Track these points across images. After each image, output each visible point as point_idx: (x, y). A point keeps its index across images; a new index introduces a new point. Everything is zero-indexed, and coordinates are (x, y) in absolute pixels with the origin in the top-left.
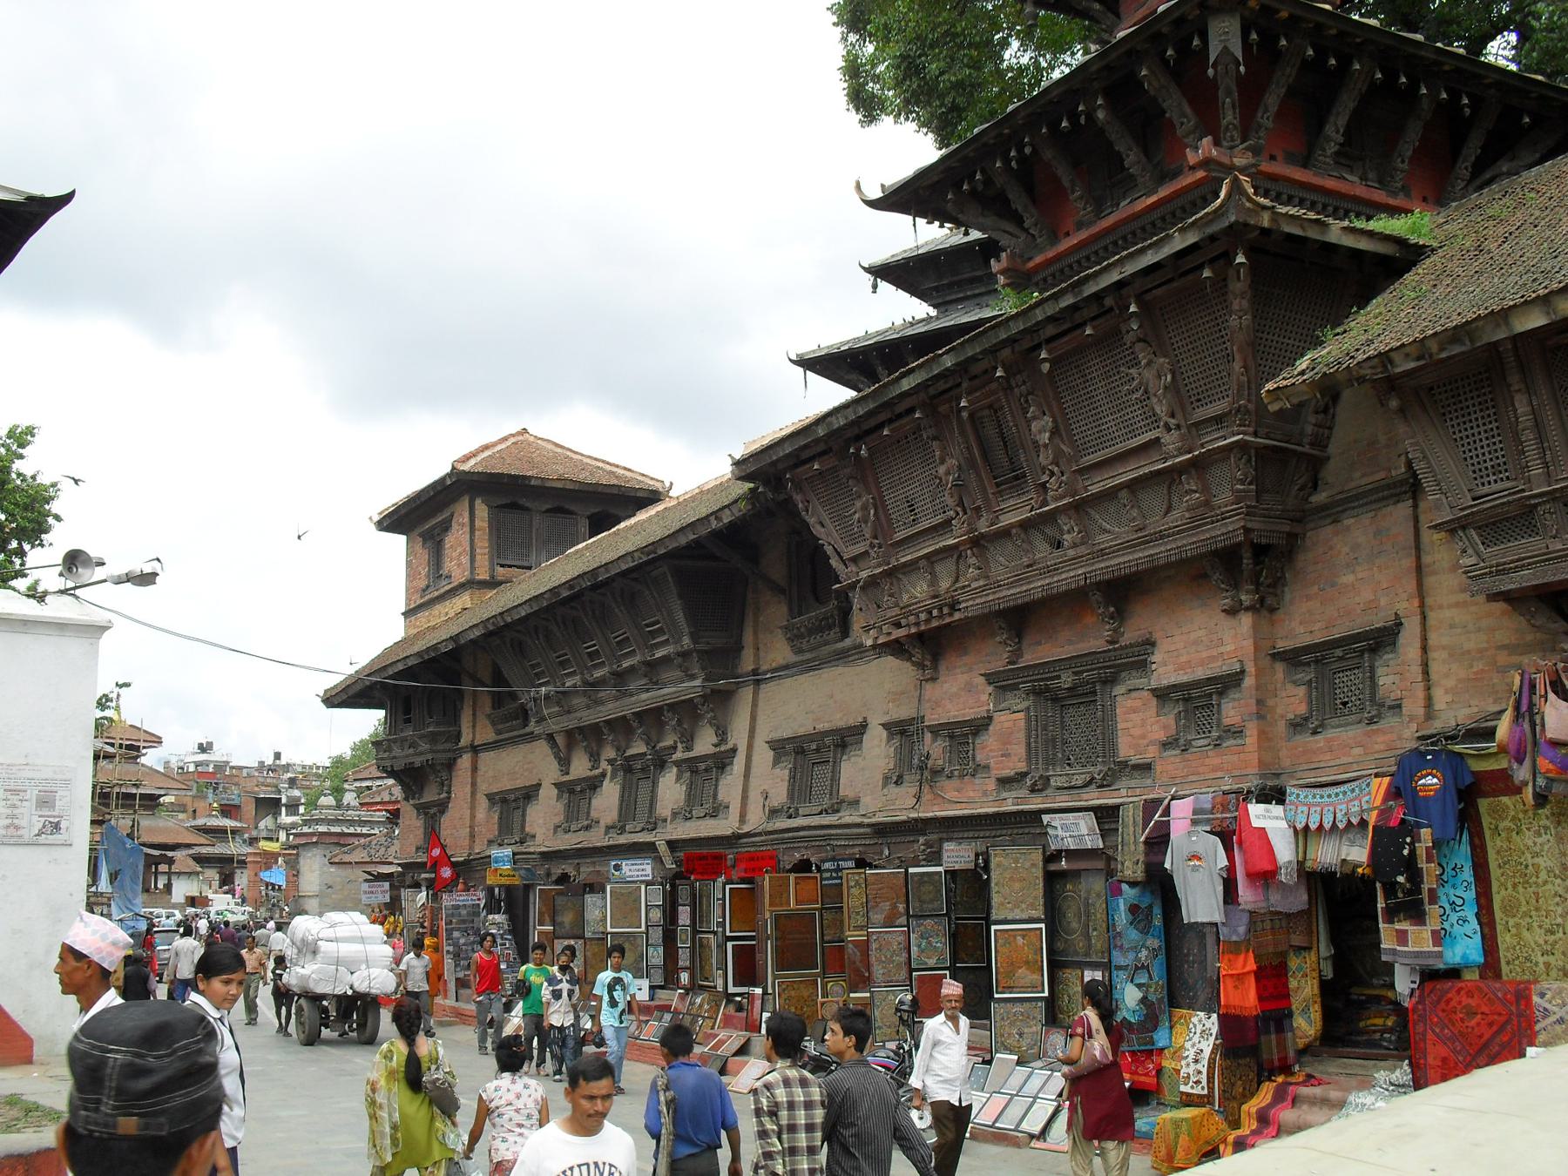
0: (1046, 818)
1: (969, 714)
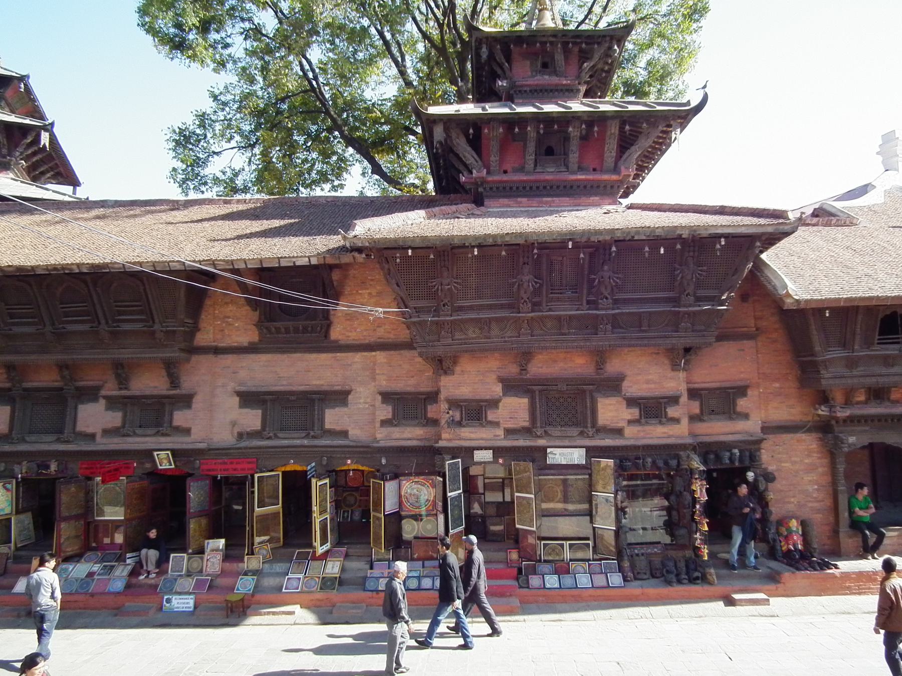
0: (549, 450)
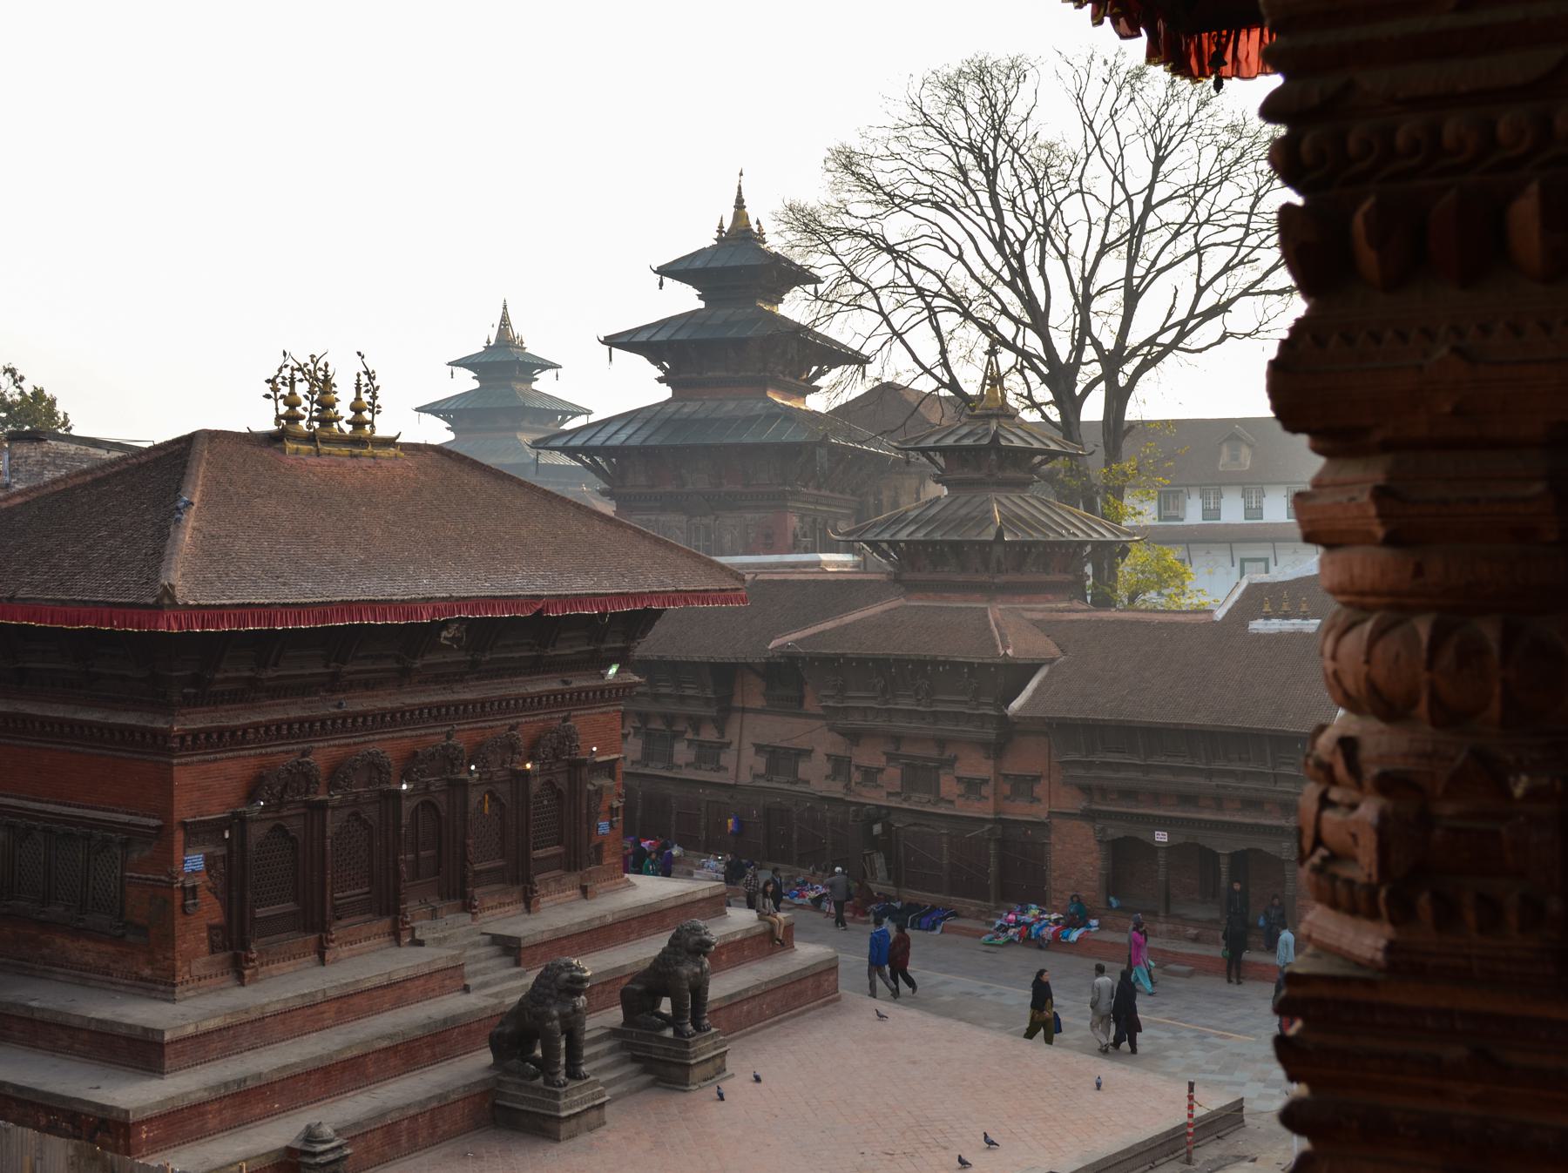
1: (876, 765)
